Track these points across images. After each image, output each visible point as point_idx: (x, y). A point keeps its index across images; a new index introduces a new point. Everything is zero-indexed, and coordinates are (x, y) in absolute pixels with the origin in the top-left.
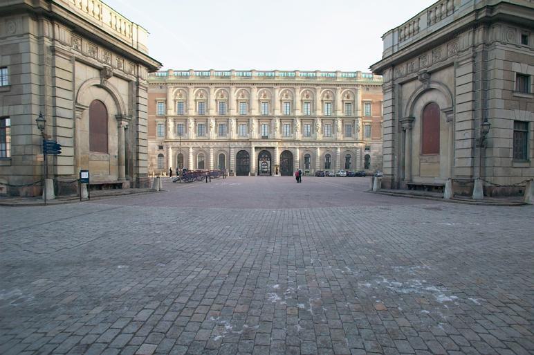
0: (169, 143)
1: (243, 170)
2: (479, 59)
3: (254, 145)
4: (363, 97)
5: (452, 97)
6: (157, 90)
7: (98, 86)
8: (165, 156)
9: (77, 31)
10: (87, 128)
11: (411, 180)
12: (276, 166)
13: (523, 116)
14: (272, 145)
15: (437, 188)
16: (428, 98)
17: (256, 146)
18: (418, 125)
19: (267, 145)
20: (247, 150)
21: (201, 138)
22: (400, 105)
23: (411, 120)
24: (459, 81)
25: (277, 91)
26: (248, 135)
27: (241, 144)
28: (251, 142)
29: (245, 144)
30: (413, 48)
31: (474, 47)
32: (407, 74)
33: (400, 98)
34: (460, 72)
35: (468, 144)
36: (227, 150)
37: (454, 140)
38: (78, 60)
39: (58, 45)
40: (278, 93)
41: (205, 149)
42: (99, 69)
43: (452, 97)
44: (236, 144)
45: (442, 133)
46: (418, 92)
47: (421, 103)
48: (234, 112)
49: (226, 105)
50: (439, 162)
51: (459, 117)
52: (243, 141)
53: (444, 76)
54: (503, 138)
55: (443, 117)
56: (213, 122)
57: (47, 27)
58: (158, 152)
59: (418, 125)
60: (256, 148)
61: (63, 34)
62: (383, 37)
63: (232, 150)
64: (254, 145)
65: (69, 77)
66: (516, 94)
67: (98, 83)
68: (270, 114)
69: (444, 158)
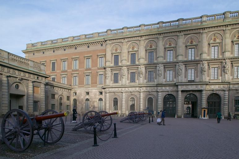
0: (107, 89)
6: (99, 47)
8: (104, 100)
12: (204, 108)
14: (199, 88)
17: (183, 89)
20: (174, 94)
21: (133, 84)
26: (175, 80)
27: (168, 88)
28: (177, 86)
29: (171, 88)
36: (155, 93)
41: (136, 94)
44: (164, 88)
49: (155, 54)
52: (169, 85)
58: (99, 97)
60: (182, 91)
64: (180, 88)
68: (197, 58)
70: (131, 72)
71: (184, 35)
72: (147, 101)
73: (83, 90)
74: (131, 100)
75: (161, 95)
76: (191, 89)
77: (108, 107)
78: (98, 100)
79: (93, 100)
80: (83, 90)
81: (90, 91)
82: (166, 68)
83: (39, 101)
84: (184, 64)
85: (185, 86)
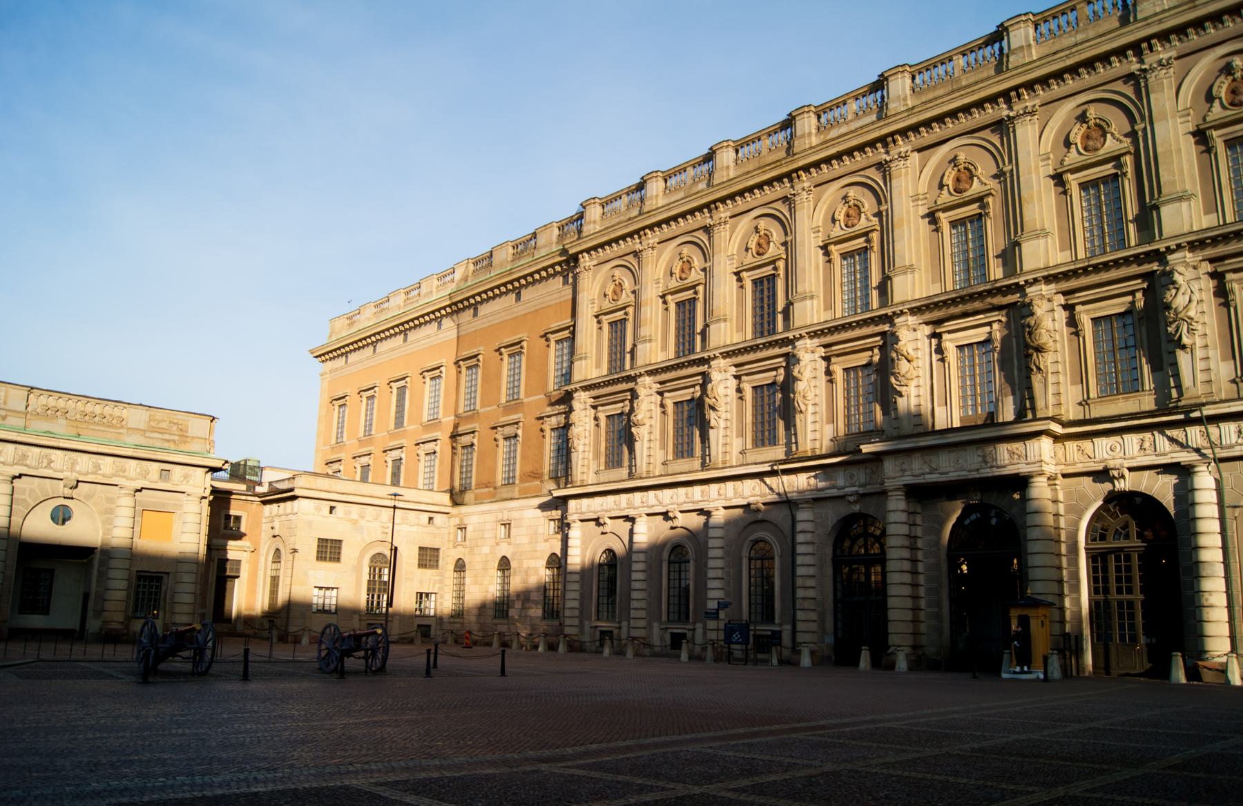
1: (859, 623)
17: (909, 480)
25: (1026, 132)
48: (810, 314)
63: (802, 515)
64: (896, 474)
70: (676, 404)
71: (919, 150)
72: (745, 562)
73: (490, 512)
74: (672, 558)
75: (809, 526)
76: (954, 476)
77: (576, 604)
78: (544, 563)
79: (525, 566)
80: (490, 512)
81: (515, 515)
82: (838, 355)
83: (168, 573)
84: (927, 323)
85: (918, 455)
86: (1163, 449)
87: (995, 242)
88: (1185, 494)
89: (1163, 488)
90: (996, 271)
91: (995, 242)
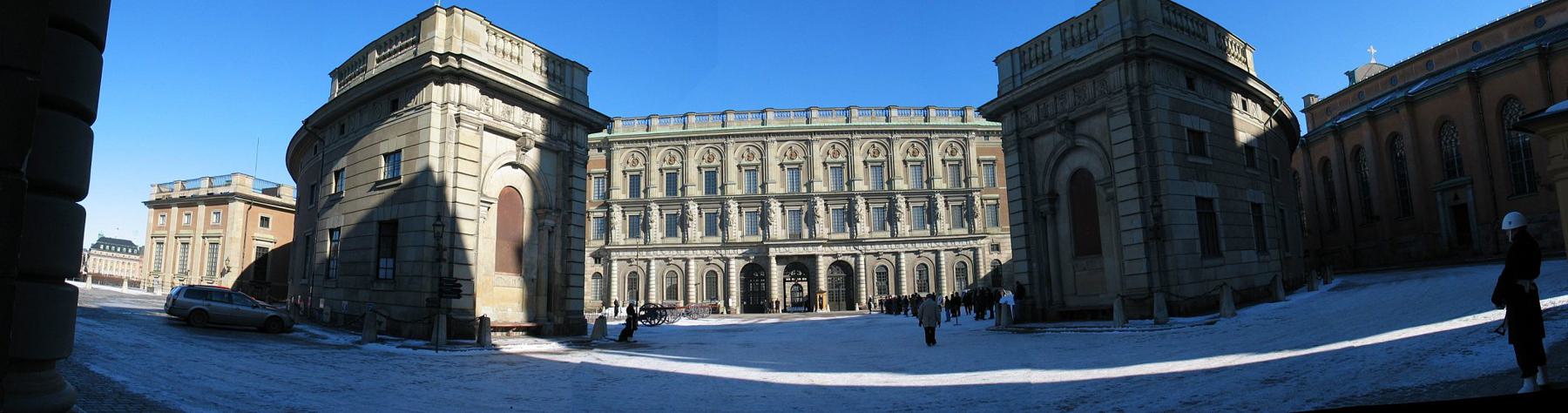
1: (756, 299)
2: (1137, 107)
3: (773, 252)
4: (979, 151)
5: (1108, 158)
7: (514, 165)
9: (489, 88)
10: (494, 234)
11: (1064, 304)
13: (1207, 190)
14: (811, 251)
15: (1104, 312)
16: (1076, 161)
18: (1064, 204)
19: (800, 251)
20: (762, 264)
22: (1033, 172)
23: (1053, 197)
24: (1116, 137)
30: (1044, 82)
31: (1128, 87)
32: (1039, 121)
33: (1032, 160)
34: (1116, 122)
35: (1139, 236)
37: (1119, 231)
38: (488, 129)
39: (464, 111)
40: (819, 150)
42: (515, 138)
43: (1108, 158)
45: (1101, 219)
46: (1060, 151)
47: (1065, 172)
48: (733, 190)
50: (1102, 269)
51: (1123, 194)
53: (1095, 125)
54: (1184, 225)
55: (1101, 193)
56: (693, 208)
57: (454, 88)
59: (1064, 204)
60: (778, 258)
61: (471, 93)
62: (997, 61)
65: (474, 155)
66: (1191, 159)
67: (513, 159)
69: (1110, 262)
86: (851, 250)
87: (803, 179)
88: (857, 262)
89: (851, 261)
90: (804, 190)
91: (803, 179)
